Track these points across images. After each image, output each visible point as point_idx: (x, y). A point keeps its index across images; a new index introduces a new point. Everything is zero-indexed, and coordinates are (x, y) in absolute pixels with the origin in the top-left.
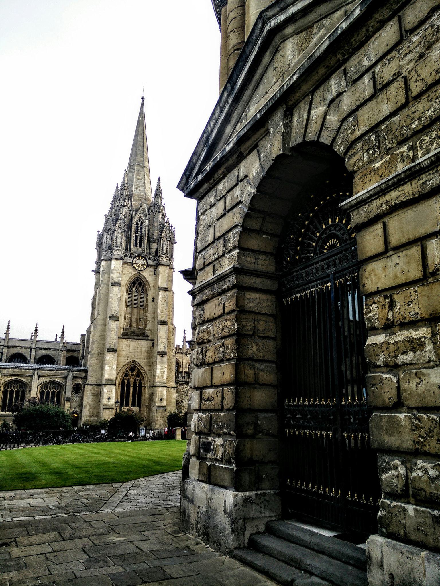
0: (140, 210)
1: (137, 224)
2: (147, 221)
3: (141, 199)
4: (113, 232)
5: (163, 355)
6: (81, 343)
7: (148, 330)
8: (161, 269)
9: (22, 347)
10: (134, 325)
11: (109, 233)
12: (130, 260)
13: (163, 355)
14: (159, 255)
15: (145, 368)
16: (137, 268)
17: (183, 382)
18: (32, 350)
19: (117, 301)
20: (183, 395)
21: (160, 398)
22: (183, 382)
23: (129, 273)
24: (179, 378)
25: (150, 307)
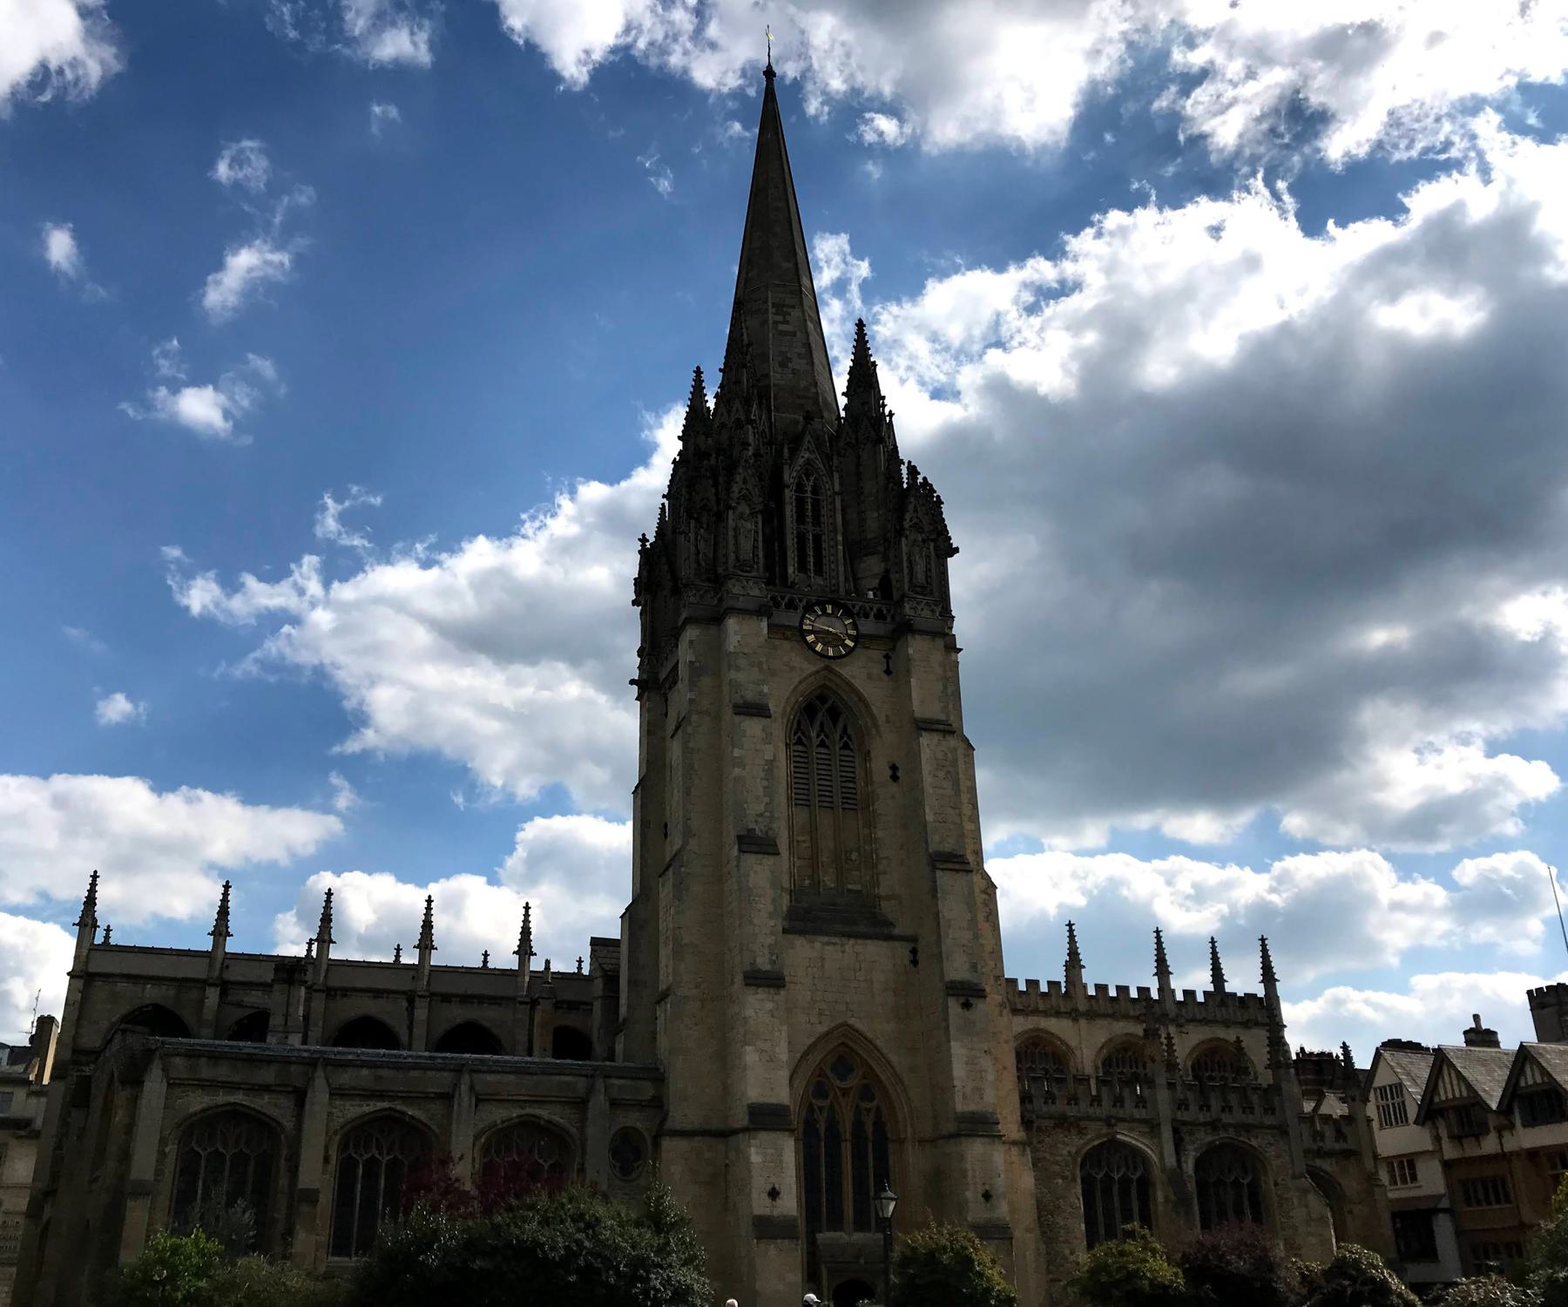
0: (808, 438)
1: (800, 488)
2: (836, 476)
3: (803, 401)
4: (720, 517)
5: (972, 1000)
6: (598, 974)
7: (888, 898)
8: (916, 647)
10: (829, 881)
11: (704, 520)
12: (791, 618)
13: (972, 1000)
14: (896, 595)
15: (894, 1058)
16: (819, 648)
17: (1051, 1117)
18: (418, 1002)
19: (762, 774)
21: (981, 1189)
22: (1051, 1117)
23: (792, 669)
24: (1031, 1102)
25: (887, 801)
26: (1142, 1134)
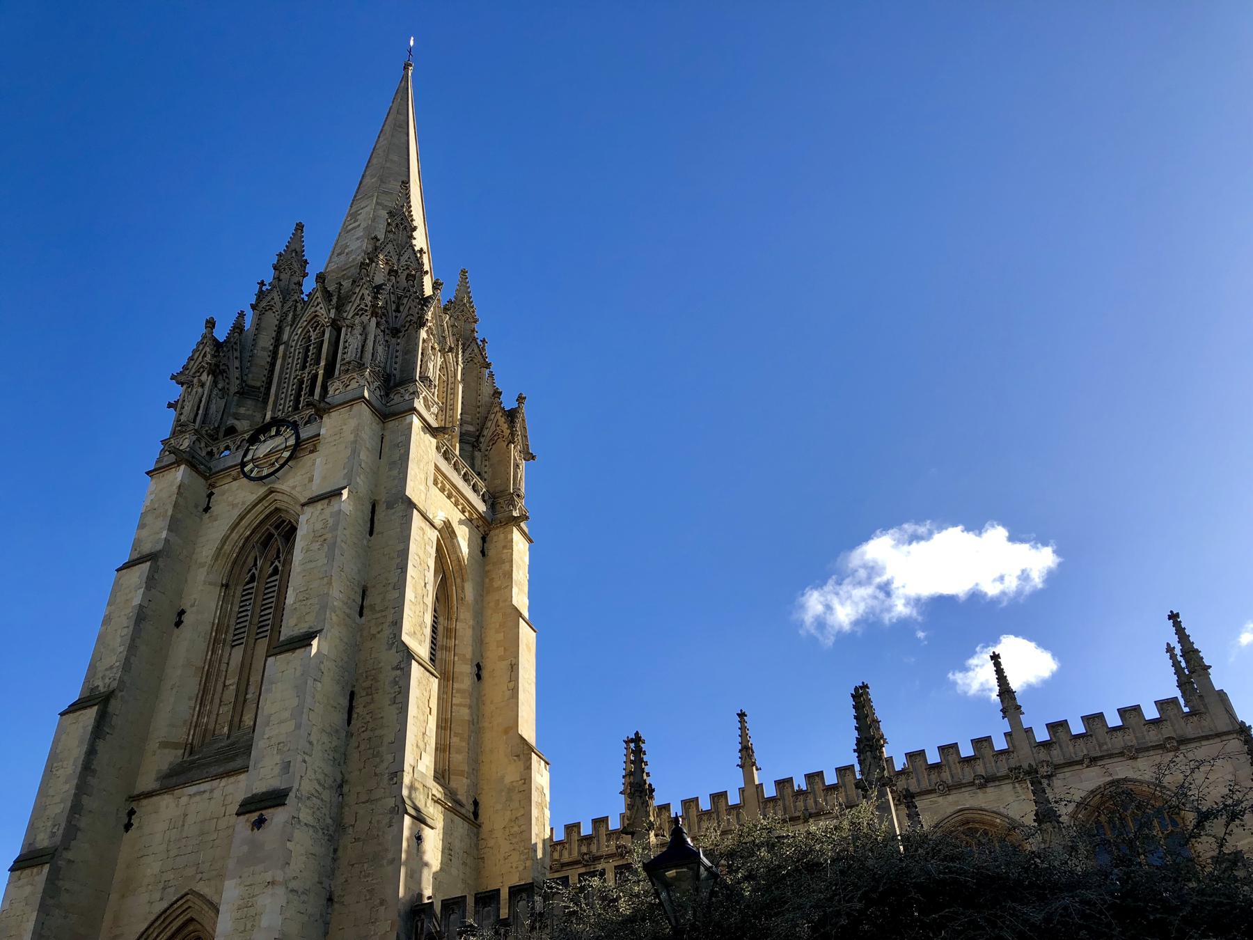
13: (267, 813)
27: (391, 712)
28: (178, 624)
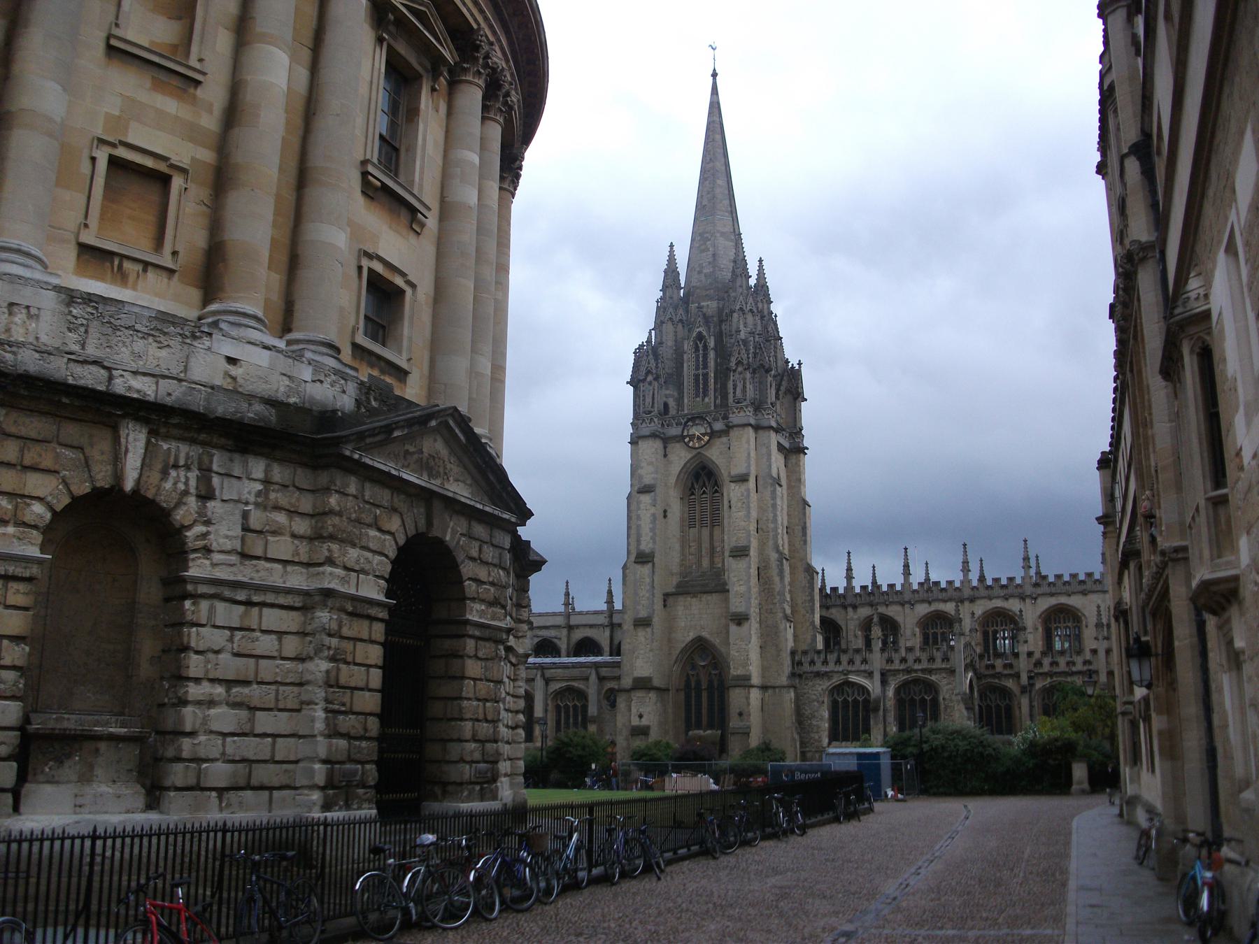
1: (697, 349)
2: (712, 338)
9: (591, 626)
16: (691, 444)
20: (814, 701)
21: (738, 711)
26: (866, 677)
27: (777, 579)
28: (665, 516)
